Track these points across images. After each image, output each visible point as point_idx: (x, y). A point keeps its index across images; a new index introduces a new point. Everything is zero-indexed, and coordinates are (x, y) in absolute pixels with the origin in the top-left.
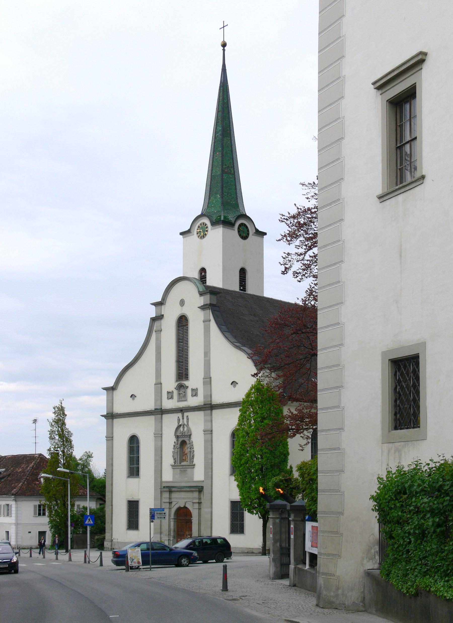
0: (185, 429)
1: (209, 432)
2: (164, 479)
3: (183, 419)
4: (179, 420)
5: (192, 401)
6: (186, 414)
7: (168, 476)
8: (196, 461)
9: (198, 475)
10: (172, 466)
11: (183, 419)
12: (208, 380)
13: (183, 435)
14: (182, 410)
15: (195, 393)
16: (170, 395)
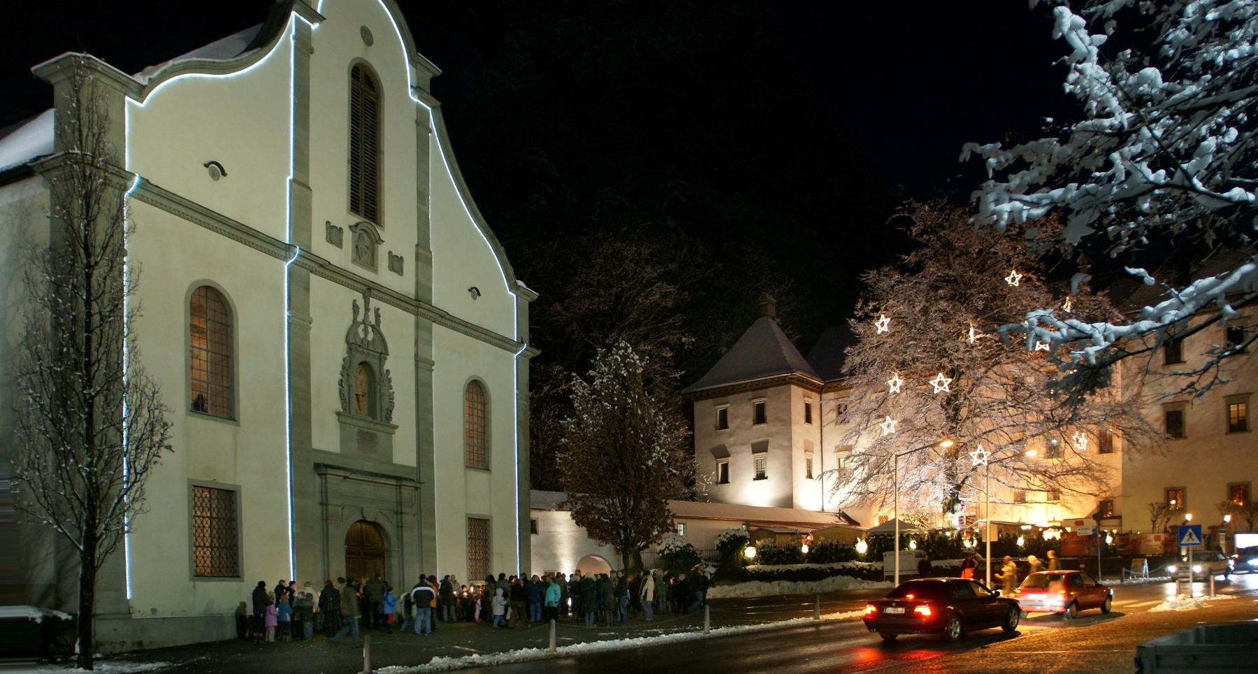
0: (370, 337)
1: (423, 365)
2: (317, 443)
3: (367, 309)
4: (355, 308)
5: (385, 277)
6: (374, 303)
7: (327, 437)
8: (396, 418)
9: (404, 452)
10: (338, 414)
11: (367, 309)
12: (423, 254)
13: (364, 344)
14: (370, 290)
15: (396, 264)
16: (334, 235)
